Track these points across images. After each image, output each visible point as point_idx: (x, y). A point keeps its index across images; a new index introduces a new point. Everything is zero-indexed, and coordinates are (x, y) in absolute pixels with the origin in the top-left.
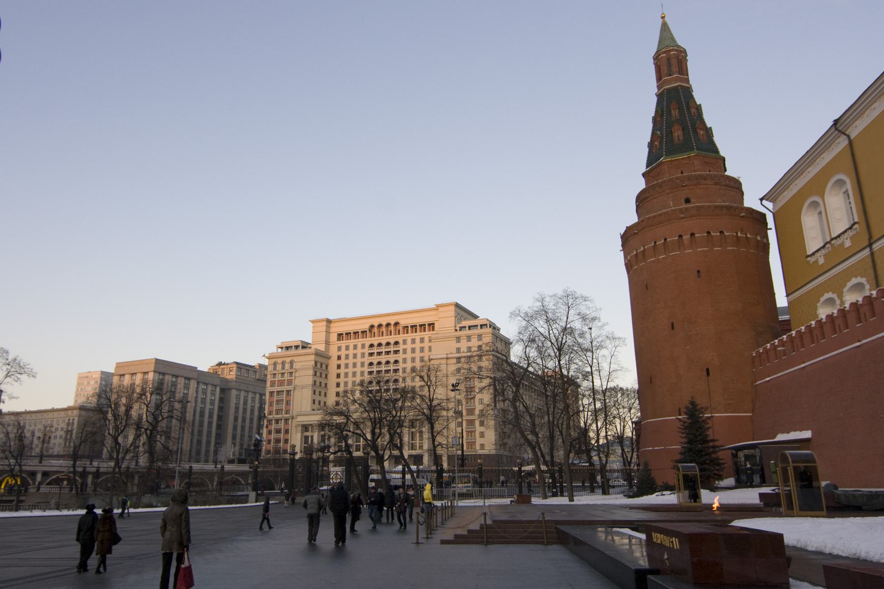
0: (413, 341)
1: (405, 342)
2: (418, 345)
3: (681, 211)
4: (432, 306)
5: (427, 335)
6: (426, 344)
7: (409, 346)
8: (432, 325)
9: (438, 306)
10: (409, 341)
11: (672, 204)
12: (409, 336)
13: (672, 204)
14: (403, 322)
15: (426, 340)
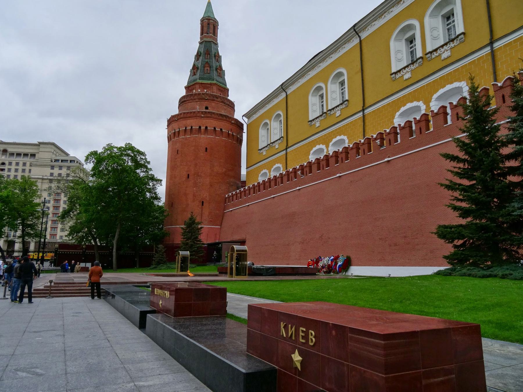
0: (17, 164)
1: (10, 164)
2: (20, 167)
3: (202, 112)
4: (35, 142)
5: (28, 160)
6: (27, 168)
7: (13, 167)
8: (33, 155)
9: (40, 144)
10: (14, 163)
11: (198, 107)
12: (14, 160)
13: (198, 107)
14: (10, 149)
15: (28, 164)
